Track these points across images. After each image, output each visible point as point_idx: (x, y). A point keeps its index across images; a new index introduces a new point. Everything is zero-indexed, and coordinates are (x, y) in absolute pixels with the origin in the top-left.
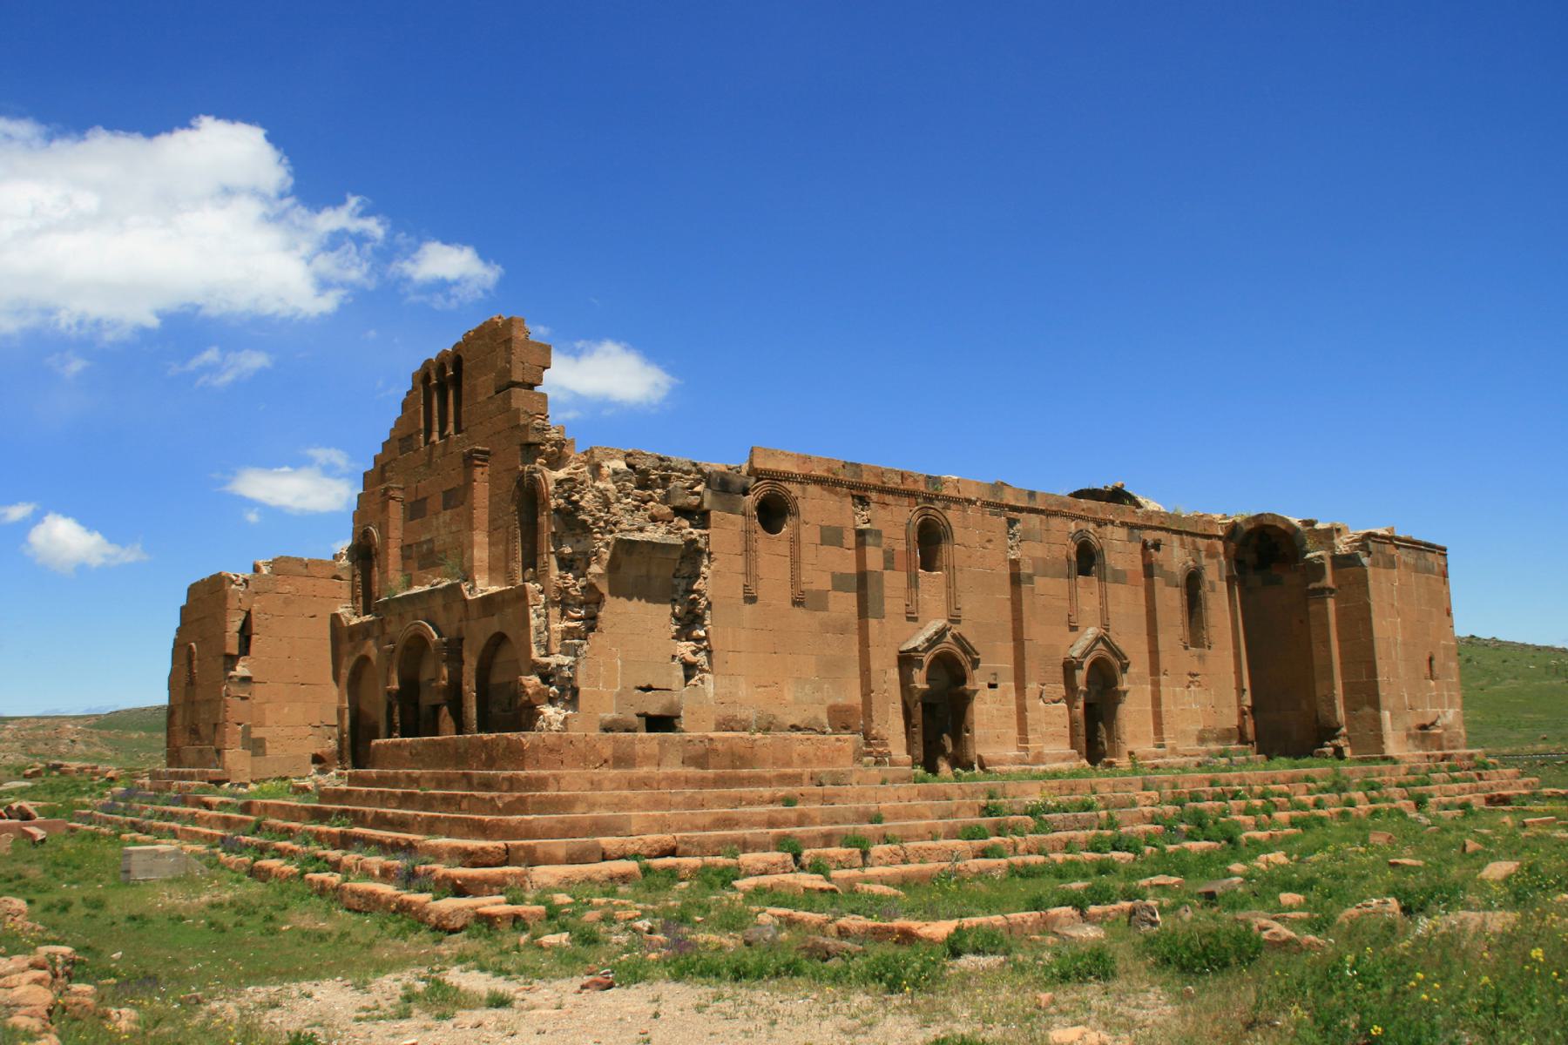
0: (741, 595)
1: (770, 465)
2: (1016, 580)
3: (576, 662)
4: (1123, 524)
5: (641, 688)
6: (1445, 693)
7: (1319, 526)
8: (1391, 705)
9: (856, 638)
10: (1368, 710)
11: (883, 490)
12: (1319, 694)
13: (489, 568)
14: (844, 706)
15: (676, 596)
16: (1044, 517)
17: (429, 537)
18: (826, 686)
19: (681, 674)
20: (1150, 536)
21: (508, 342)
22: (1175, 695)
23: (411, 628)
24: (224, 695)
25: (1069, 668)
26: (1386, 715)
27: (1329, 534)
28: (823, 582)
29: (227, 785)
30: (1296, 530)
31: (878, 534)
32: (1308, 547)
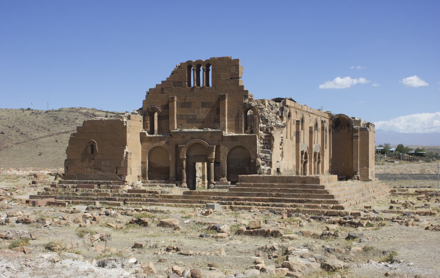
2: (311, 132)
3: (272, 155)
7: (356, 119)
9: (294, 148)
10: (366, 168)
12: (354, 162)
13: (228, 127)
20: (323, 119)
21: (237, 66)
23: (196, 141)
24: (124, 158)
25: (315, 154)
26: (369, 169)
27: (359, 121)
30: (350, 120)
32: (353, 124)
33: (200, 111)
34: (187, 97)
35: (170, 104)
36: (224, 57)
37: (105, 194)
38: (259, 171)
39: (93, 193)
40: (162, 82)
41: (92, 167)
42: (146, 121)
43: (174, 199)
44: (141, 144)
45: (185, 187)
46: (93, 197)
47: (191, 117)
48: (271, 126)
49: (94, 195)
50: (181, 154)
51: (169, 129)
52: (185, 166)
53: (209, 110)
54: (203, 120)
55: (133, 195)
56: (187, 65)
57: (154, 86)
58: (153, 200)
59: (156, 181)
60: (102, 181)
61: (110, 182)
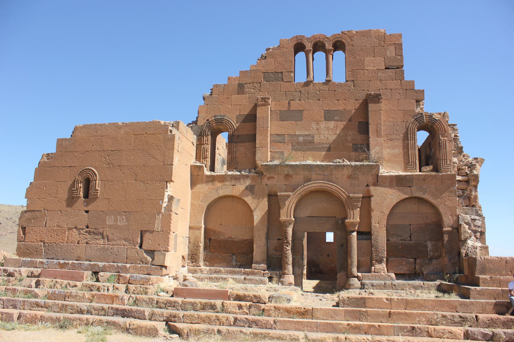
17: (307, 134)
21: (399, 47)
23: (318, 185)
24: (163, 211)
29: (167, 276)
33: (323, 128)
34: (294, 100)
35: (259, 110)
36: (370, 30)
37: (113, 299)
38: (464, 251)
39: (80, 293)
40: (241, 72)
41: (83, 229)
42: (203, 144)
43: (317, 318)
44: (192, 189)
45: (290, 284)
46: (78, 304)
47: (301, 139)
48: (468, 162)
49: (82, 299)
50: (283, 212)
51: (255, 161)
52: (290, 239)
53: (341, 125)
54: (328, 146)
55: (193, 304)
56: (295, 43)
57: (224, 81)
58: (259, 320)
59: (222, 269)
60: (103, 263)
61: (125, 266)
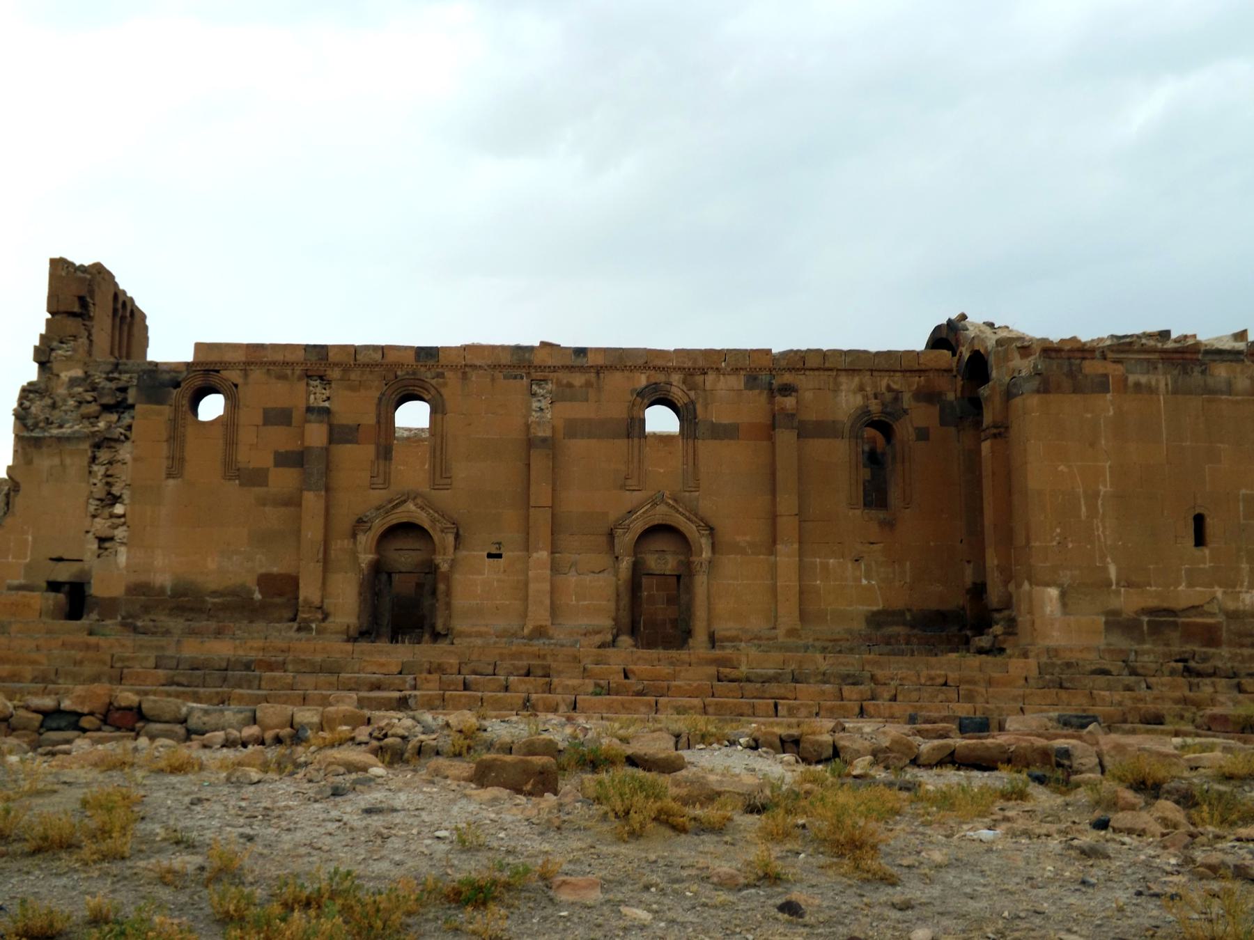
0: (164, 476)
1: (214, 357)
4: (736, 370)
5: (52, 559)
6: (1245, 566)
8: (1066, 581)
11: (346, 369)
14: (280, 575)
15: (95, 481)
16: (627, 373)
18: (258, 556)
19: (95, 546)
22: (825, 567)
28: (264, 459)
30: (988, 353)
31: (327, 411)
32: (994, 374)
